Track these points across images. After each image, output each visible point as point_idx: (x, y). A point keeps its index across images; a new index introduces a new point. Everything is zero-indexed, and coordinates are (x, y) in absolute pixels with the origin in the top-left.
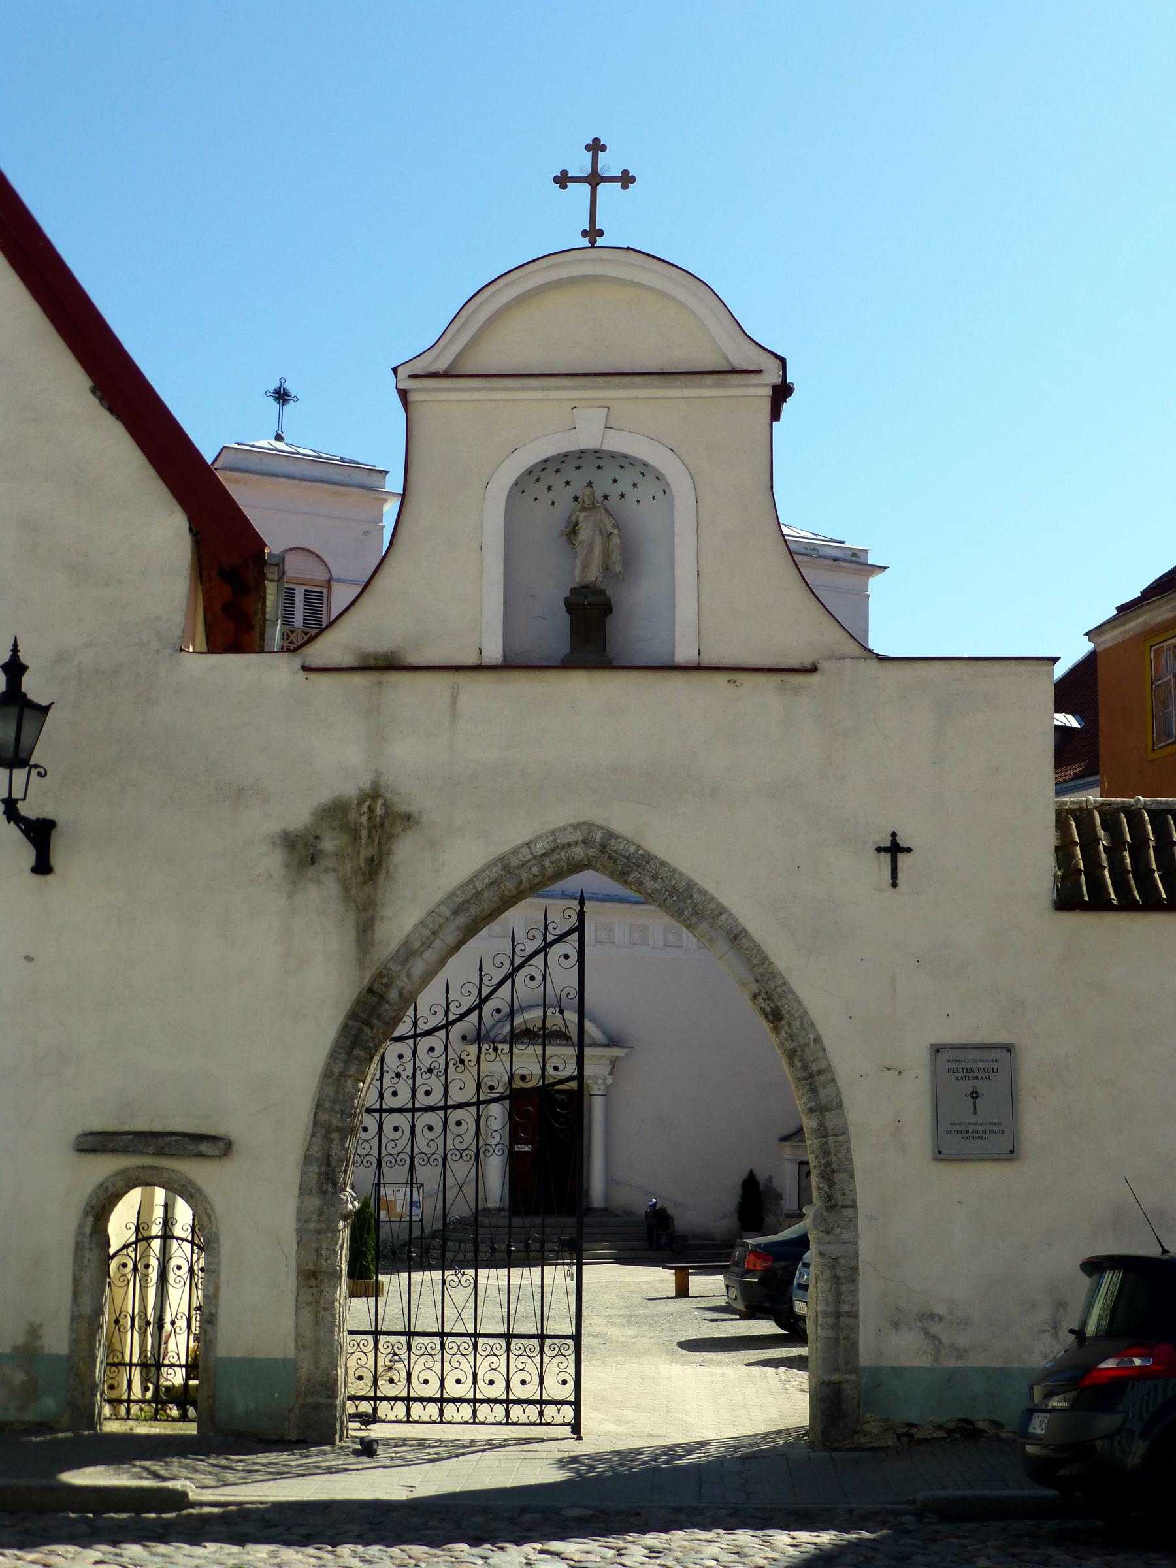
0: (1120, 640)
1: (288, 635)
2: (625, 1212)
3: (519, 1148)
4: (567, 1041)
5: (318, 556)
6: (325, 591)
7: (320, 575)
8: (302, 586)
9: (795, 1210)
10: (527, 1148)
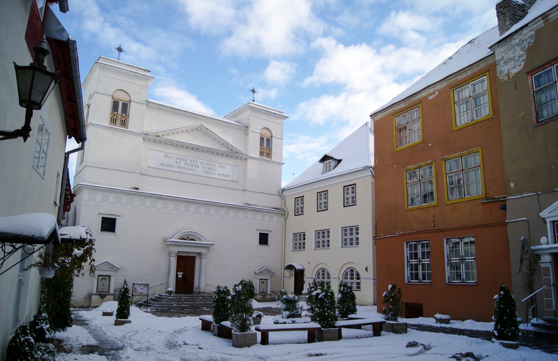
0: (383, 116)
2: (210, 293)
5: (127, 93)
6: (129, 103)
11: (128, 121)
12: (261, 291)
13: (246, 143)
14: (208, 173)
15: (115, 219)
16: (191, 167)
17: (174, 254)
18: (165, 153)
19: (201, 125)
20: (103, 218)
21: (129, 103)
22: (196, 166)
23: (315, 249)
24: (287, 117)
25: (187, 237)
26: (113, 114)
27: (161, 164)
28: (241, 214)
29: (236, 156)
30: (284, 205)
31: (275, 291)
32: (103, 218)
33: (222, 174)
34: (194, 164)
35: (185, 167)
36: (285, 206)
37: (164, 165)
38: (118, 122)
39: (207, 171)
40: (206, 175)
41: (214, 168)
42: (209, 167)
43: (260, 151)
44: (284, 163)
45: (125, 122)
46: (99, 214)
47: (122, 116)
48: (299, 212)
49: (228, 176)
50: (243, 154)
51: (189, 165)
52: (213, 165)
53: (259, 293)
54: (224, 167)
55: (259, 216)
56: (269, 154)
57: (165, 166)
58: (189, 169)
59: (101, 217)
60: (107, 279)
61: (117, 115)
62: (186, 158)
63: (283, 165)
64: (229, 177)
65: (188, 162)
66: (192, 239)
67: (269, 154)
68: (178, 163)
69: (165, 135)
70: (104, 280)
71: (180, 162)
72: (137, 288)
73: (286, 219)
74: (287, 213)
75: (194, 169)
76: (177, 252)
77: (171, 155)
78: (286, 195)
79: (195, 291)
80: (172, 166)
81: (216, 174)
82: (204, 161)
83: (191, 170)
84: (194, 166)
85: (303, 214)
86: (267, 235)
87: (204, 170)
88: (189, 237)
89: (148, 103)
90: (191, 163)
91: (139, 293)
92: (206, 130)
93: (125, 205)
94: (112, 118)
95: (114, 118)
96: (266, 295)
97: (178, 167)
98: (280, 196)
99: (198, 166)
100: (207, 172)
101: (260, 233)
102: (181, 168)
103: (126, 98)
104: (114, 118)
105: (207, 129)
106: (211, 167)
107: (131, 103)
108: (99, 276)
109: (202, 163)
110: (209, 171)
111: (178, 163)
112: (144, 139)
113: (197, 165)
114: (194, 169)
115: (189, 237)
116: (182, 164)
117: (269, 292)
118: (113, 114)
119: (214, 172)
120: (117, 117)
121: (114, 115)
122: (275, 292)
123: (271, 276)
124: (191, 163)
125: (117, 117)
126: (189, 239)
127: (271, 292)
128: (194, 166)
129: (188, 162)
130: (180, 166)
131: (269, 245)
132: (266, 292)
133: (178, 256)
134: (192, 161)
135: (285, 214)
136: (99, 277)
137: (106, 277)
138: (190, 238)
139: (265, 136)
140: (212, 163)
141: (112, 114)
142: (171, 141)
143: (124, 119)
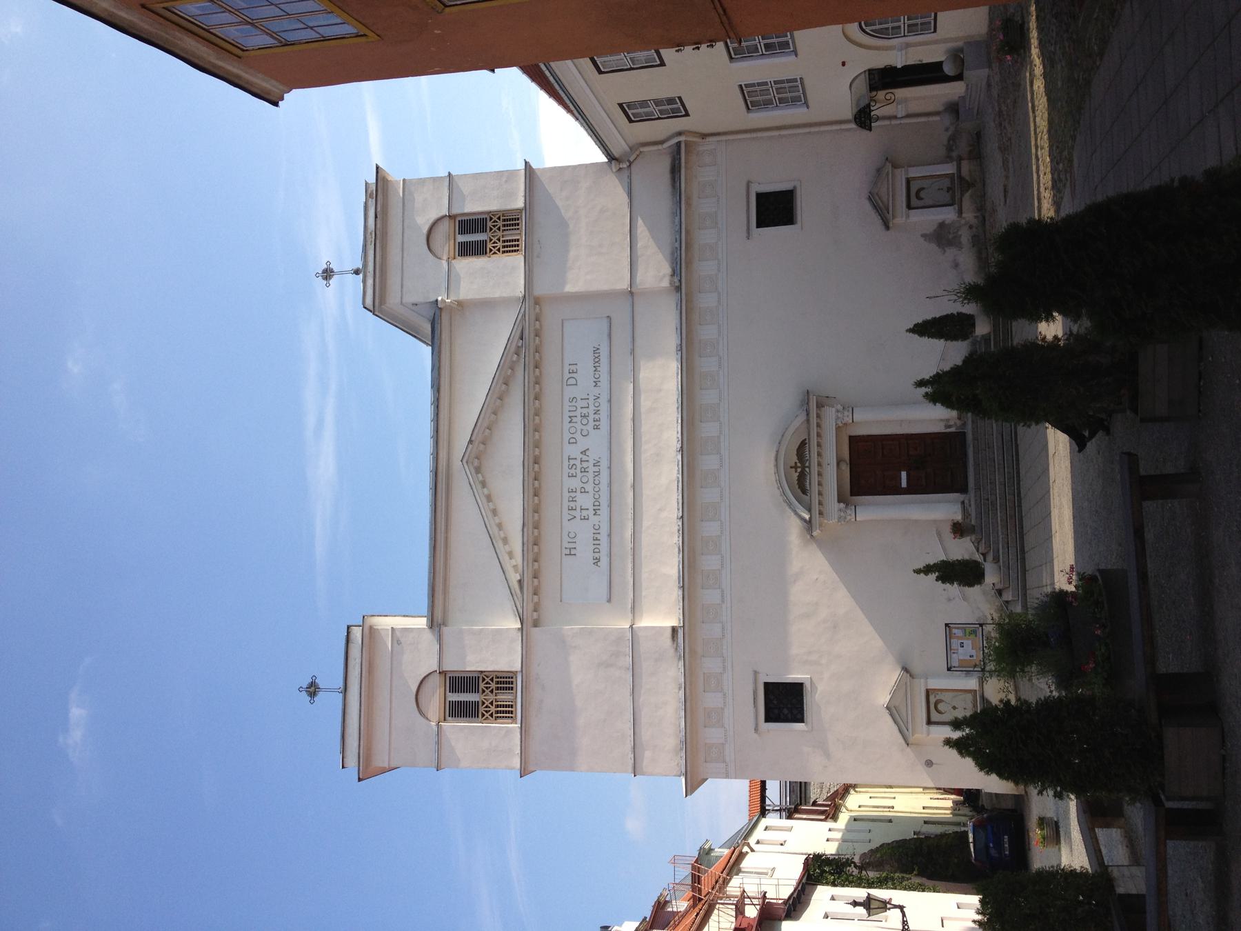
1: (487, 707)
3: (904, 484)
4: (806, 444)
7: (436, 680)
8: (447, 695)
9: (955, 209)
10: (904, 474)
11: (496, 673)
12: (946, 197)
13: (487, 305)
14: (597, 417)
15: (767, 685)
16: (591, 475)
17: (849, 512)
18: (563, 555)
19: (464, 461)
20: (768, 719)
22: (585, 458)
24: (377, 172)
25: (794, 469)
26: (487, 715)
28: (706, 301)
29: (532, 335)
30: (660, 147)
31: (946, 143)
32: (768, 719)
33: (592, 373)
34: (579, 466)
35: (592, 492)
36: (662, 142)
37: (597, 555)
38: (504, 697)
39: (591, 423)
40: (604, 423)
42: (579, 418)
43: (504, 252)
44: (526, 162)
45: (499, 680)
46: (756, 730)
47: (487, 691)
49: (596, 350)
50: (524, 315)
51: (585, 480)
52: (573, 403)
53: (956, 206)
54: (573, 367)
55: (705, 237)
58: (596, 478)
60: (938, 697)
61: (487, 703)
62: (565, 491)
63: (530, 166)
64: (598, 349)
65: (575, 483)
68: (585, 513)
69: (513, 562)
70: (941, 707)
71: (581, 509)
72: (961, 658)
73: (704, 136)
76: (842, 505)
77: (566, 539)
78: (623, 143)
79: (956, 429)
80: (597, 530)
81: (596, 391)
82: (567, 436)
83: (597, 474)
84: (585, 465)
85: (680, 98)
86: (760, 197)
87: (592, 432)
88: (793, 465)
89: (435, 624)
90: (579, 475)
91: (974, 651)
92: (476, 443)
93: (724, 661)
96: (961, 178)
97: (594, 514)
98: (631, 163)
99: (584, 453)
100: (597, 423)
101: (759, 225)
102: (597, 503)
103: (436, 685)
105: (471, 441)
106: (579, 410)
107: (444, 670)
108: (929, 722)
109: (572, 441)
111: (585, 513)
112: (536, 624)
113: (579, 456)
115: (793, 465)
116: (585, 501)
117: (949, 169)
118: (487, 715)
119: (591, 402)
120: (492, 703)
122: (949, 141)
123: (895, 166)
124: (579, 475)
125: (492, 703)
126: (799, 465)
127: (948, 159)
128: (585, 465)
129: (575, 483)
130: (591, 508)
131: (795, 187)
132: (951, 176)
133: (852, 495)
134: (573, 471)
136: (933, 719)
137: (932, 700)
138: (795, 459)
139: (455, 240)
140: (566, 408)
142: (525, 546)
143: (493, 685)
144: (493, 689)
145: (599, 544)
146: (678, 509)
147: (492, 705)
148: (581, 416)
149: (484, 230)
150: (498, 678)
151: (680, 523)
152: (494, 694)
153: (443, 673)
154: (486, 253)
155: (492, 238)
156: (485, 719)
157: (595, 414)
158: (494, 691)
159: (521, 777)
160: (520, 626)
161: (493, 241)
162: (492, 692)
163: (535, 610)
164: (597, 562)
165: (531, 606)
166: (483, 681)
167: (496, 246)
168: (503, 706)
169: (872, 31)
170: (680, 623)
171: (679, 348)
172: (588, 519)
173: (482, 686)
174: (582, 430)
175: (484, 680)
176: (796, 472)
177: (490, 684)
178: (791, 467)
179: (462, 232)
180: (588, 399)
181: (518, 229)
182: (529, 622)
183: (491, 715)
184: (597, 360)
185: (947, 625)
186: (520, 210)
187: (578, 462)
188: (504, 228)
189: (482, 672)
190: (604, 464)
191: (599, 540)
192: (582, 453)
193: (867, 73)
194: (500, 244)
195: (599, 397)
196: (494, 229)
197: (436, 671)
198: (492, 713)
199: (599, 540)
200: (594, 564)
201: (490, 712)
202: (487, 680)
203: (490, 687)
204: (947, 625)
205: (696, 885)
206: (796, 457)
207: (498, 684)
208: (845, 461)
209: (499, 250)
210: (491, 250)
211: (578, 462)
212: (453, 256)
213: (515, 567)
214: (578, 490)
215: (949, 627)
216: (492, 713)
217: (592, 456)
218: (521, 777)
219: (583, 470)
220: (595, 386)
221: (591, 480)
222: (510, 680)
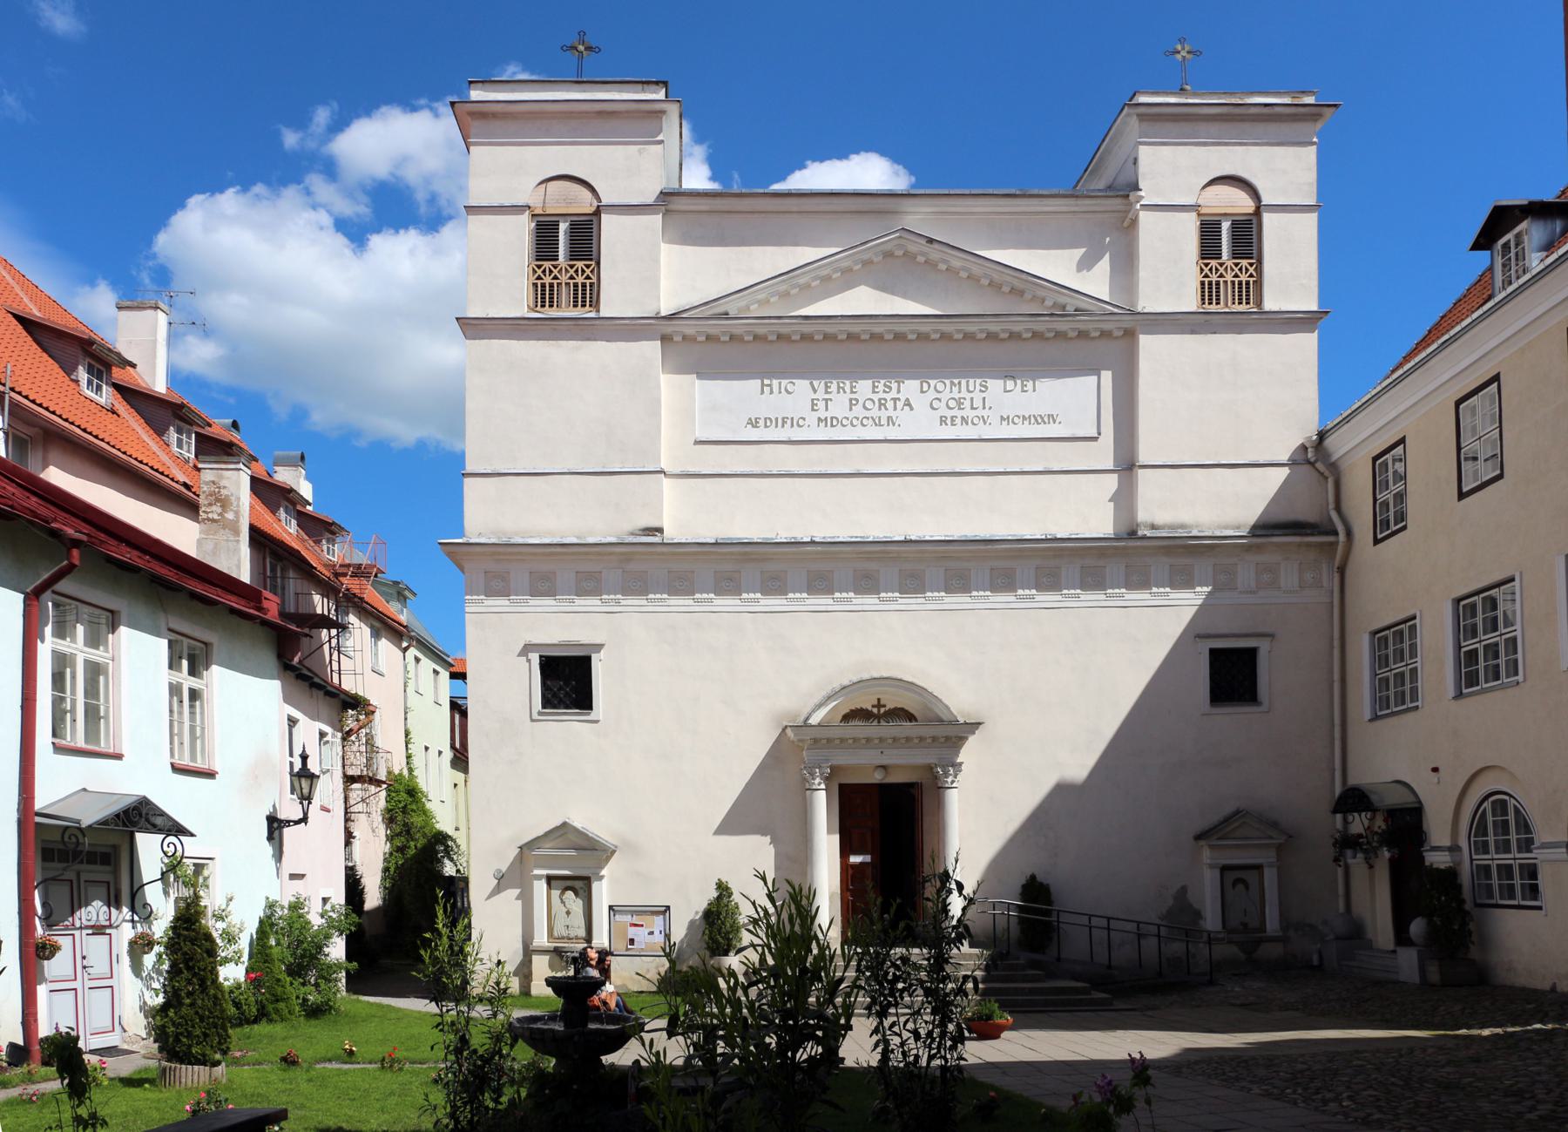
14: (958, 421)
16: (875, 413)
21: (594, 218)
22: (900, 404)
23: (1459, 695)
25: (876, 703)
26: (539, 272)
27: (750, 422)
33: (1020, 414)
34: (888, 396)
37: (761, 423)
39: (949, 414)
41: (984, 395)
42: (957, 396)
43: (1203, 283)
47: (572, 272)
48: (1390, 521)
56: (1248, 288)
57: (766, 426)
59: (535, 658)
61: (555, 272)
66: (896, 709)
67: (1248, 288)
68: (821, 405)
74: (1342, 537)
75: (889, 418)
81: (994, 419)
84: (890, 404)
88: (882, 703)
90: (875, 397)
94: (535, 285)
95: (543, 286)
97: (819, 419)
99: (908, 403)
100: (949, 422)
102: (835, 423)
103: (583, 203)
104: (543, 286)
106: (968, 396)
110: (959, 413)
111: (821, 405)
114: (889, 418)
115: (882, 703)
118: (539, 272)
119: (980, 412)
120: (555, 278)
121: (551, 271)
124: (875, 397)
125: (555, 278)
126: (882, 710)
128: (890, 404)
130: (829, 415)
135: (1334, 545)
138: (890, 706)
141: (535, 272)
144: (575, 279)
145: (777, 426)
146: (824, 538)
147: (585, 279)
148: (960, 398)
149: (1235, 255)
150: (590, 286)
151: (805, 540)
152: (569, 281)
153: (597, 213)
154: (1203, 258)
155: (1224, 266)
156: (533, 269)
157: (963, 418)
158: (572, 282)
159: (457, 319)
160: (663, 314)
161: (1249, 267)
162: (572, 278)
163: (685, 338)
164: (752, 424)
165: (690, 331)
166: (585, 265)
167: (1212, 273)
168: (551, 294)
169: (1485, 809)
170: (668, 539)
171: (1049, 537)
172: (813, 410)
173: (580, 264)
174: (940, 400)
175: (588, 266)
176: (873, 706)
177: (582, 275)
178: (879, 700)
179: (1236, 226)
180: (984, 408)
181: (1234, 303)
182: (669, 328)
183: (539, 278)
184: (1040, 421)
185: (668, 908)
186: (1259, 303)
187: (893, 394)
188: (1236, 283)
189: (598, 264)
190: (892, 433)
191: (783, 426)
192: (907, 400)
193: (1417, 805)
194: (1214, 278)
195: (985, 423)
196: (1236, 269)
197: (601, 202)
198: (542, 279)
199: (783, 426)
200: (750, 419)
201: (543, 276)
202: (588, 271)
203: (545, 275)
204: (668, 908)
205: (351, 569)
206: (892, 707)
207: (582, 286)
208: (885, 777)
209: (1206, 276)
210: (1206, 265)
211: (893, 394)
212: (1202, 212)
213: (748, 308)
214: (853, 396)
215: (665, 911)
216: (542, 279)
217: (902, 415)
218: (457, 319)
219: (883, 402)
220: (1002, 417)
221: (868, 414)
222: (588, 303)
